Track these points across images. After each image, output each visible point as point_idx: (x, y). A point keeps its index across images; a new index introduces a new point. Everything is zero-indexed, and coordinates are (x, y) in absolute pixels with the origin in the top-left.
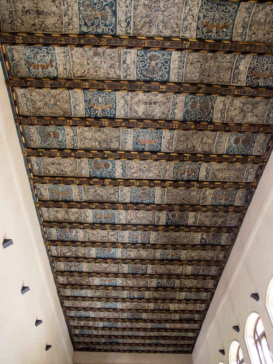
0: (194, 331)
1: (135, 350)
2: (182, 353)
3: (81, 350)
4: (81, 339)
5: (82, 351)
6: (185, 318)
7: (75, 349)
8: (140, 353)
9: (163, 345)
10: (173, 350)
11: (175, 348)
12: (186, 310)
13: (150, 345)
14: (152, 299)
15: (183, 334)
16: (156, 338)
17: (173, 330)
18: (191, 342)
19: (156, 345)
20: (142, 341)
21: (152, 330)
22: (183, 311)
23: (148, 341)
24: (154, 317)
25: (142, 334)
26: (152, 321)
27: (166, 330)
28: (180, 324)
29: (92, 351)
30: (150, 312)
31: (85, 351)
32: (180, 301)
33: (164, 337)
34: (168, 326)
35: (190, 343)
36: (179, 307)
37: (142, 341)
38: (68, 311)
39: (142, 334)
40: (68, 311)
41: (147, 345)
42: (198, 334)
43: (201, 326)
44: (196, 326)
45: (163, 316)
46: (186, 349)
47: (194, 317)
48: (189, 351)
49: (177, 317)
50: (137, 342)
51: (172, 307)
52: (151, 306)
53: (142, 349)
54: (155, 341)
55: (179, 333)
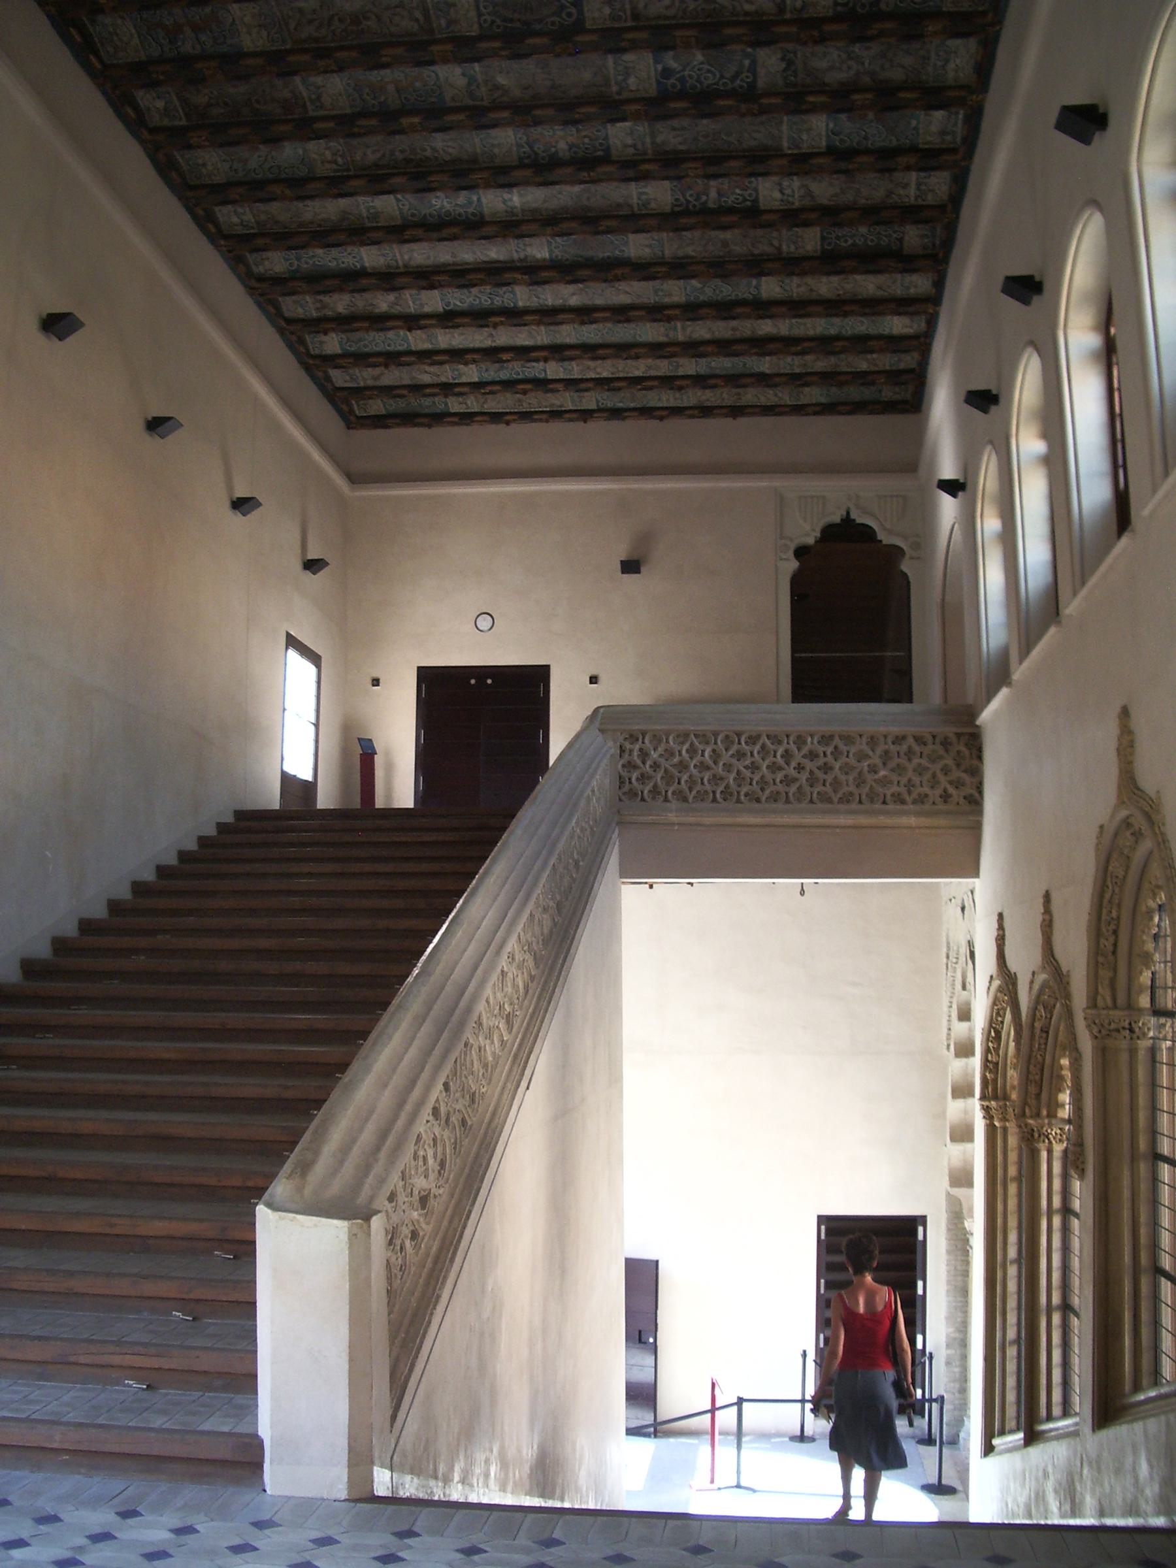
0: (912, 309)
1: (635, 409)
2: (871, 413)
3: (379, 422)
4: (365, 376)
5: (387, 427)
6: (854, 245)
7: (352, 422)
8: (661, 419)
9: (763, 379)
10: (823, 400)
11: (834, 390)
12: (848, 208)
13: (700, 380)
14: (649, 161)
15: (858, 325)
16: (723, 346)
17: (797, 307)
18: (908, 361)
19: (734, 380)
20: (663, 367)
21: (692, 310)
22: (830, 214)
23: (689, 366)
24: (690, 251)
25: (650, 332)
26: (679, 268)
27: (762, 308)
28: (835, 279)
29: (429, 426)
30: (660, 228)
31: (398, 425)
32: (801, 163)
33: (760, 345)
34: (770, 287)
35: (902, 366)
36: (809, 193)
37: (663, 367)
38: (251, 258)
39: (650, 332)
40: (251, 258)
41: (688, 382)
42: (932, 322)
43: (939, 284)
44: (920, 284)
45: (735, 241)
46: (888, 393)
47: (901, 240)
48: (905, 402)
49: (810, 240)
50: (637, 373)
51: (770, 191)
52: (659, 193)
53: (672, 403)
54: (723, 364)
55: (837, 321)
